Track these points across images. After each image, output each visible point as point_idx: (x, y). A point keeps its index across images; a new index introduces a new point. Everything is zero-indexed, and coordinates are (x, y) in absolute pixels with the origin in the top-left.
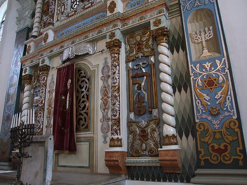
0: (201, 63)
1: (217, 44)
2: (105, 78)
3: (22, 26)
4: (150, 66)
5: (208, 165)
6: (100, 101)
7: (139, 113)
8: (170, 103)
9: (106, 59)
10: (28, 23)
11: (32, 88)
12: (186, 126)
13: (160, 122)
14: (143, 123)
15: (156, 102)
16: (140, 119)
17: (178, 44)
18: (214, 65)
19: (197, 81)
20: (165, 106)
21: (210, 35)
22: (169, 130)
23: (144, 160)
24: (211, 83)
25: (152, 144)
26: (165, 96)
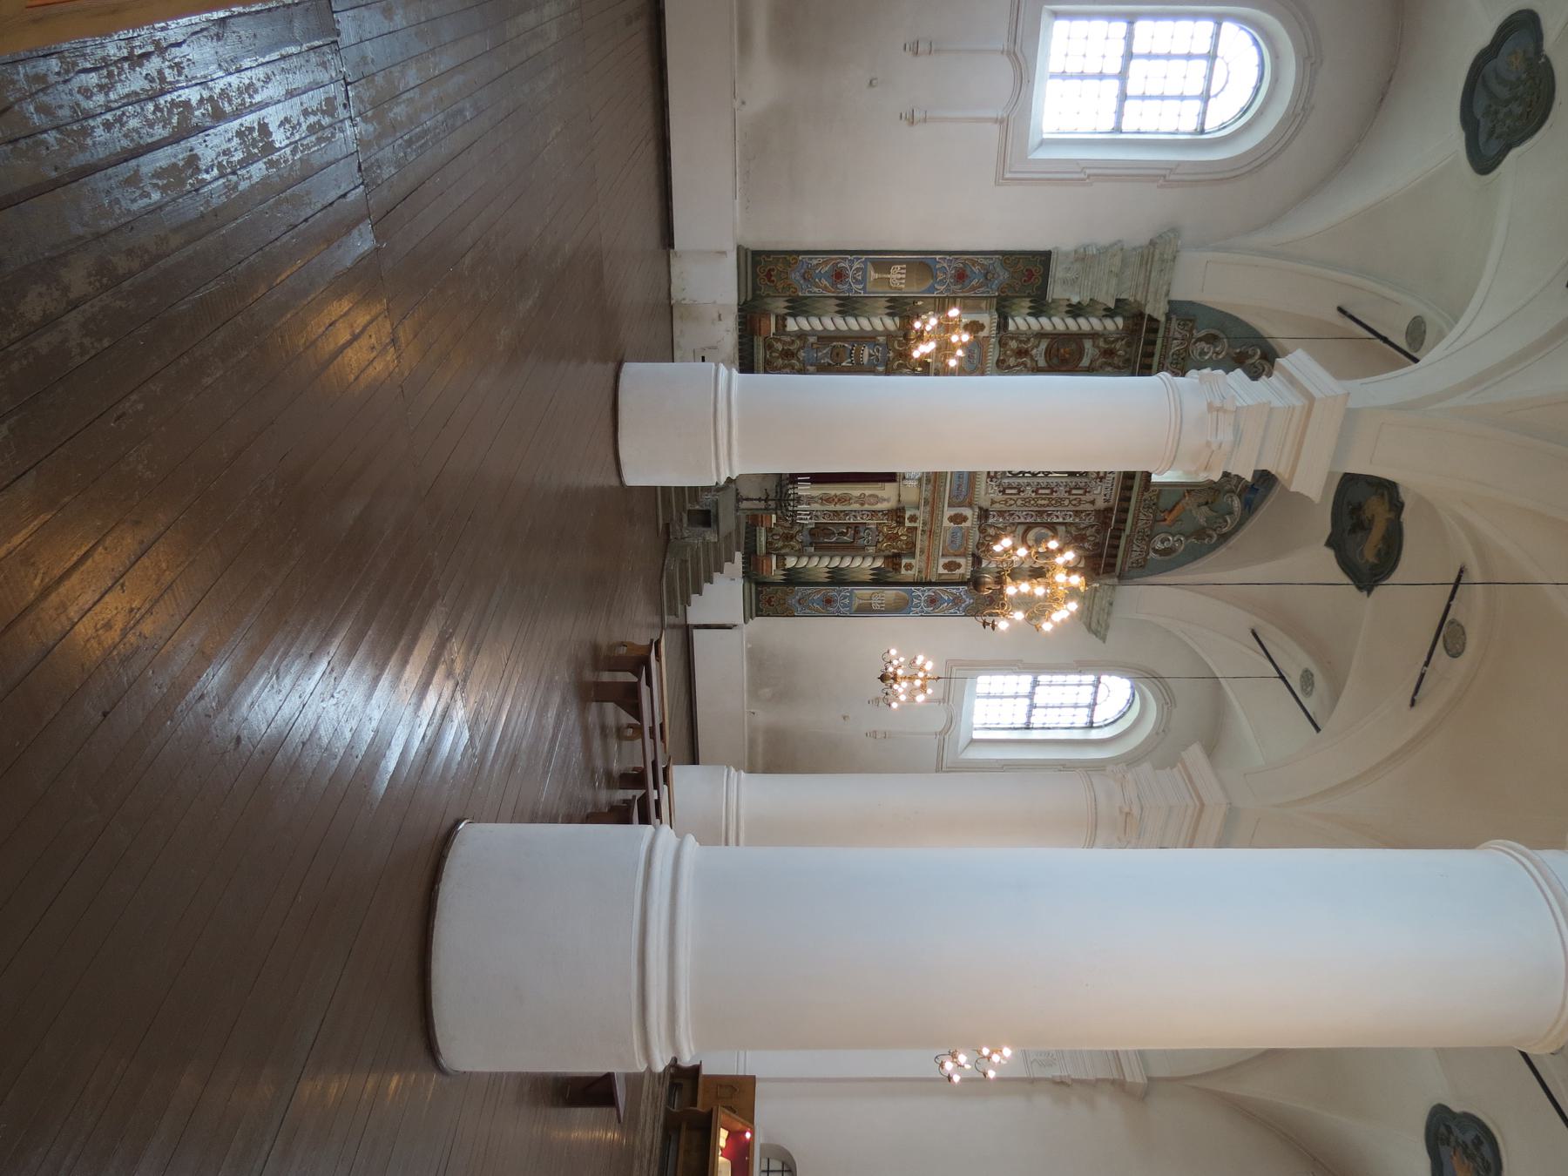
0: (850, 598)
1: (866, 610)
2: (861, 500)
3: (1058, 271)
4: (863, 548)
5: (758, 593)
6: (833, 493)
7: (812, 533)
8: (819, 565)
9: (888, 500)
10: (1056, 291)
11: (889, 335)
12: (793, 579)
13: (799, 554)
14: (800, 538)
15: (822, 549)
16: (806, 532)
17: (879, 580)
18: (845, 606)
19: (832, 591)
20: (815, 561)
21: (875, 606)
22: (791, 562)
23: (762, 539)
24: (829, 601)
25: (780, 544)
26: (826, 561)
